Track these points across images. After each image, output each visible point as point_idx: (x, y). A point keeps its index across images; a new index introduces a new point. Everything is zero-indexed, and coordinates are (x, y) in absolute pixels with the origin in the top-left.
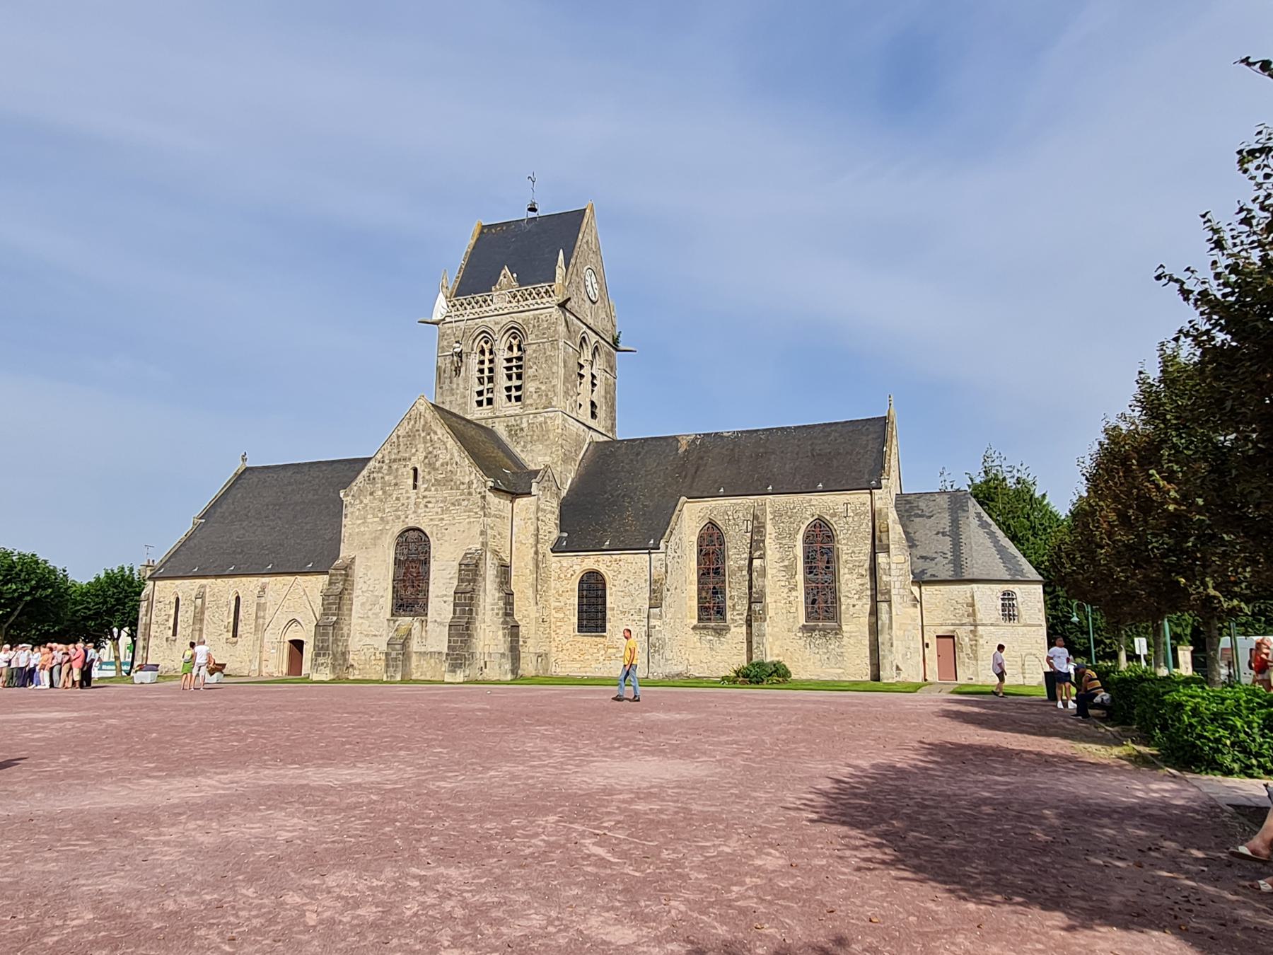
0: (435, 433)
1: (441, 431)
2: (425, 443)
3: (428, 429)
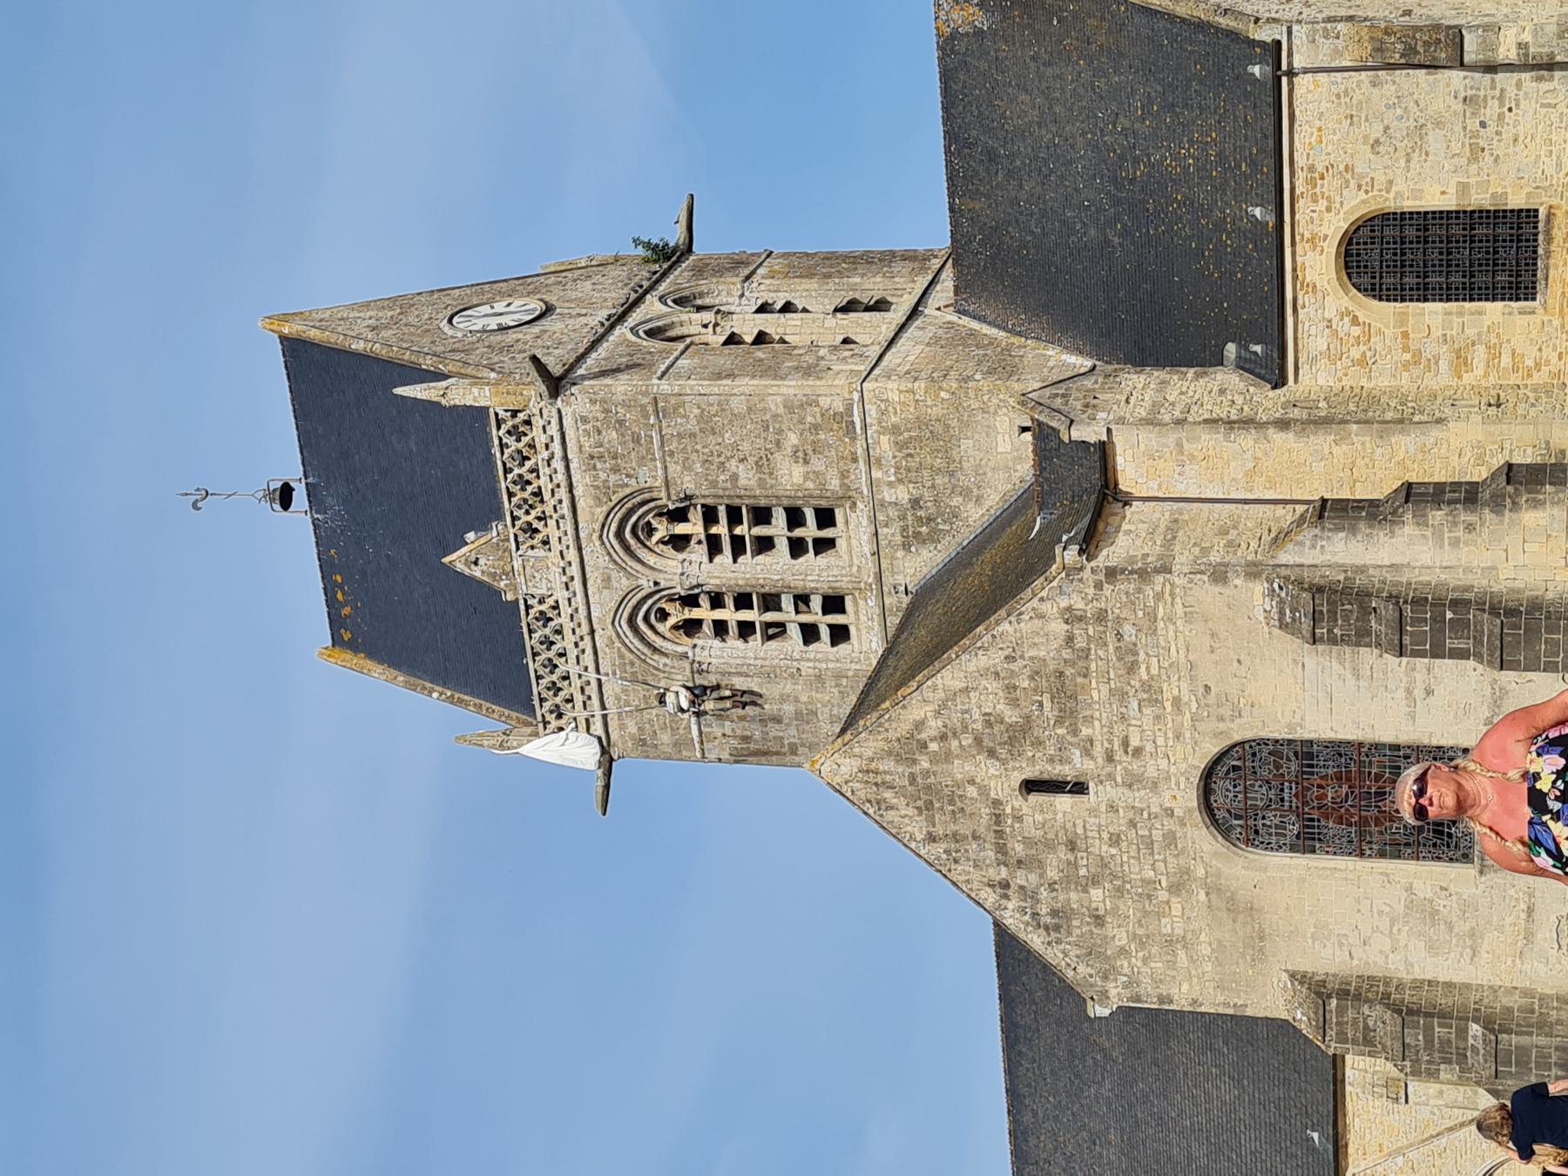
0: (919, 725)
1: (919, 708)
2: (948, 757)
3: (910, 747)
